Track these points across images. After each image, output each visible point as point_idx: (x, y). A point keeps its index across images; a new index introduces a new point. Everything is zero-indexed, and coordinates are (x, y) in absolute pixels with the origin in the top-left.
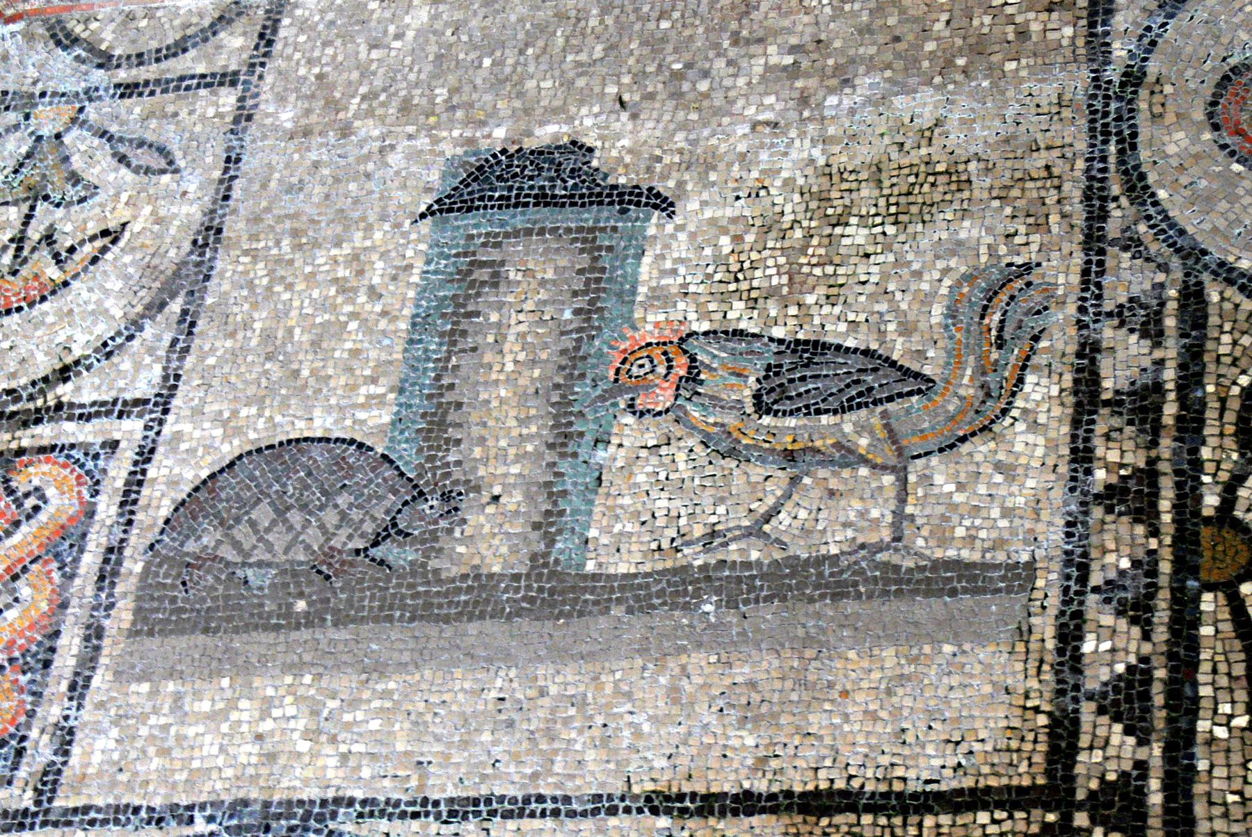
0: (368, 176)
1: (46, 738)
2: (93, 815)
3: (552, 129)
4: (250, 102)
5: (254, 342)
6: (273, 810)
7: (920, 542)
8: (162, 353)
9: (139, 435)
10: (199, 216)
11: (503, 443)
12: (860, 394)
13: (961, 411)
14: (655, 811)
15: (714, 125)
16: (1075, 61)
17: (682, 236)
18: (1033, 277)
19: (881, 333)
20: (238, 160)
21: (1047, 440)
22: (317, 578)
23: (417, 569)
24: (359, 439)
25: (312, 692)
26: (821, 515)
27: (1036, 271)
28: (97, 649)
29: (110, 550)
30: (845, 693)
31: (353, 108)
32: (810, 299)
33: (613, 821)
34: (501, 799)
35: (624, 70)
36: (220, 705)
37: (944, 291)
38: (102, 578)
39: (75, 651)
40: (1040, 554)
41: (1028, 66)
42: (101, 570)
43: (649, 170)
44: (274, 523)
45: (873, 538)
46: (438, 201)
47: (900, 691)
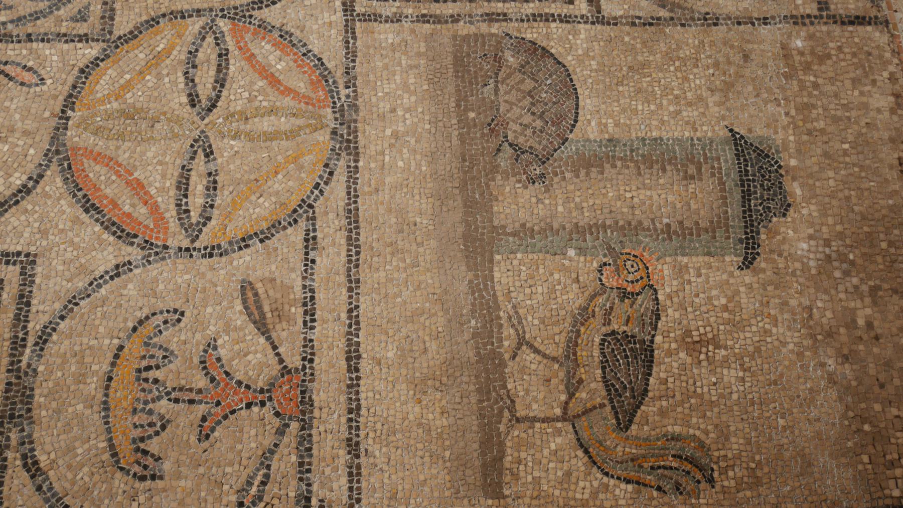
0: (758, 95)
1: (394, 10)
2: (352, 41)
3: (798, 192)
4: (807, 21)
5: (640, 58)
6: (352, 125)
7: (516, 433)
8: (631, 13)
9: (577, 13)
10: (725, 11)
11: (577, 200)
12: (616, 390)
13: (606, 449)
14: (350, 311)
15: (807, 283)
16: (872, 499)
17: (725, 277)
18: (703, 485)
19: (660, 398)
20: (766, 24)
21: (587, 500)
22: (489, 120)
23: (495, 169)
24: (577, 124)
25: (420, 130)
26: (534, 378)
27: (708, 485)
28: (446, 22)
29: (505, 15)
30: (419, 401)
31: (807, 78)
32: (682, 355)
33: (344, 291)
34: (358, 234)
35: (846, 226)
36: (412, 88)
37: (691, 431)
38: (487, 14)
39: (444, 12)
40: (509, 500)
41: (866, 470)
42: (493, 14)
43: (772, 251)
44: (524, 92)
45: (518, 406)
46: (742, 137)
47: (420, 431)
